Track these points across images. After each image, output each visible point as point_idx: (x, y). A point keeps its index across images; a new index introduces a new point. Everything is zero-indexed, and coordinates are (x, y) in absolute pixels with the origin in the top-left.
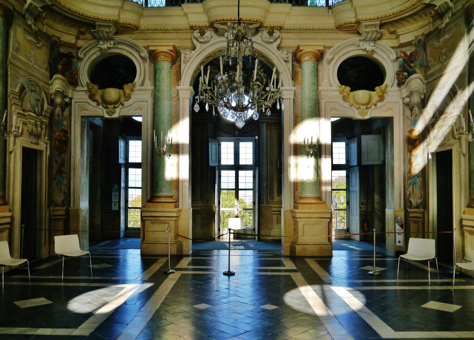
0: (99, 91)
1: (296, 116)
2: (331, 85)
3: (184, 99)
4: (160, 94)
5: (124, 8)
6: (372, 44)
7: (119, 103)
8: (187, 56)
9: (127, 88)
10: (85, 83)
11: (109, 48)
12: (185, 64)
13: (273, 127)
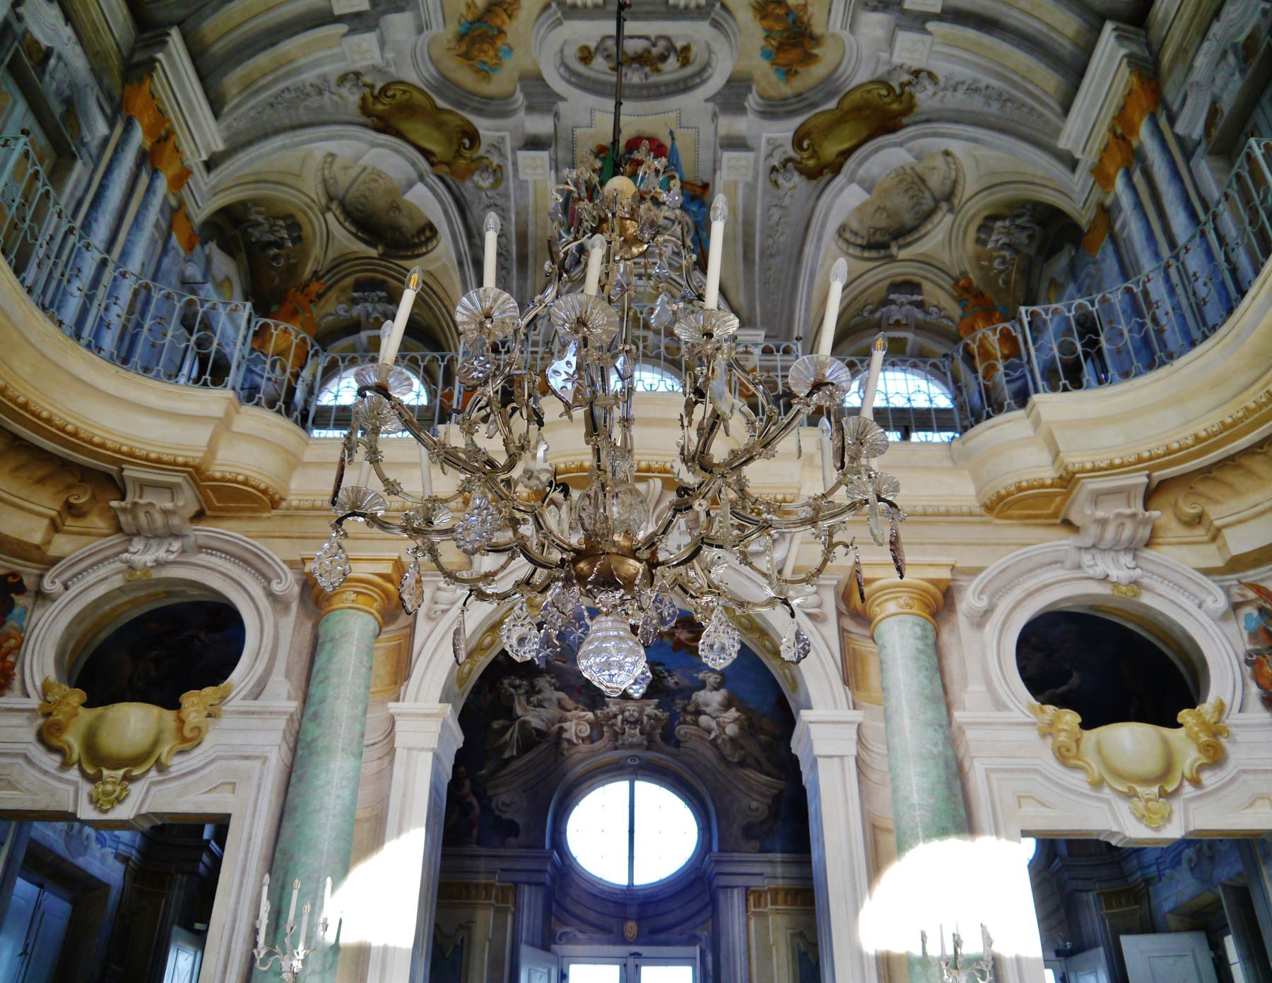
0: (82, 710)
1: (874, 827)
2: (1000, 706)
3: (415, 753)
4: (318, 732)
5: (235, 428)
6: (1126, 559)
7: (152, 761)
8: (442, 595)
9: (194, 702)
10: (38, 683)
11: (159, 564)
12: (433, 624)
13: (770, 906)
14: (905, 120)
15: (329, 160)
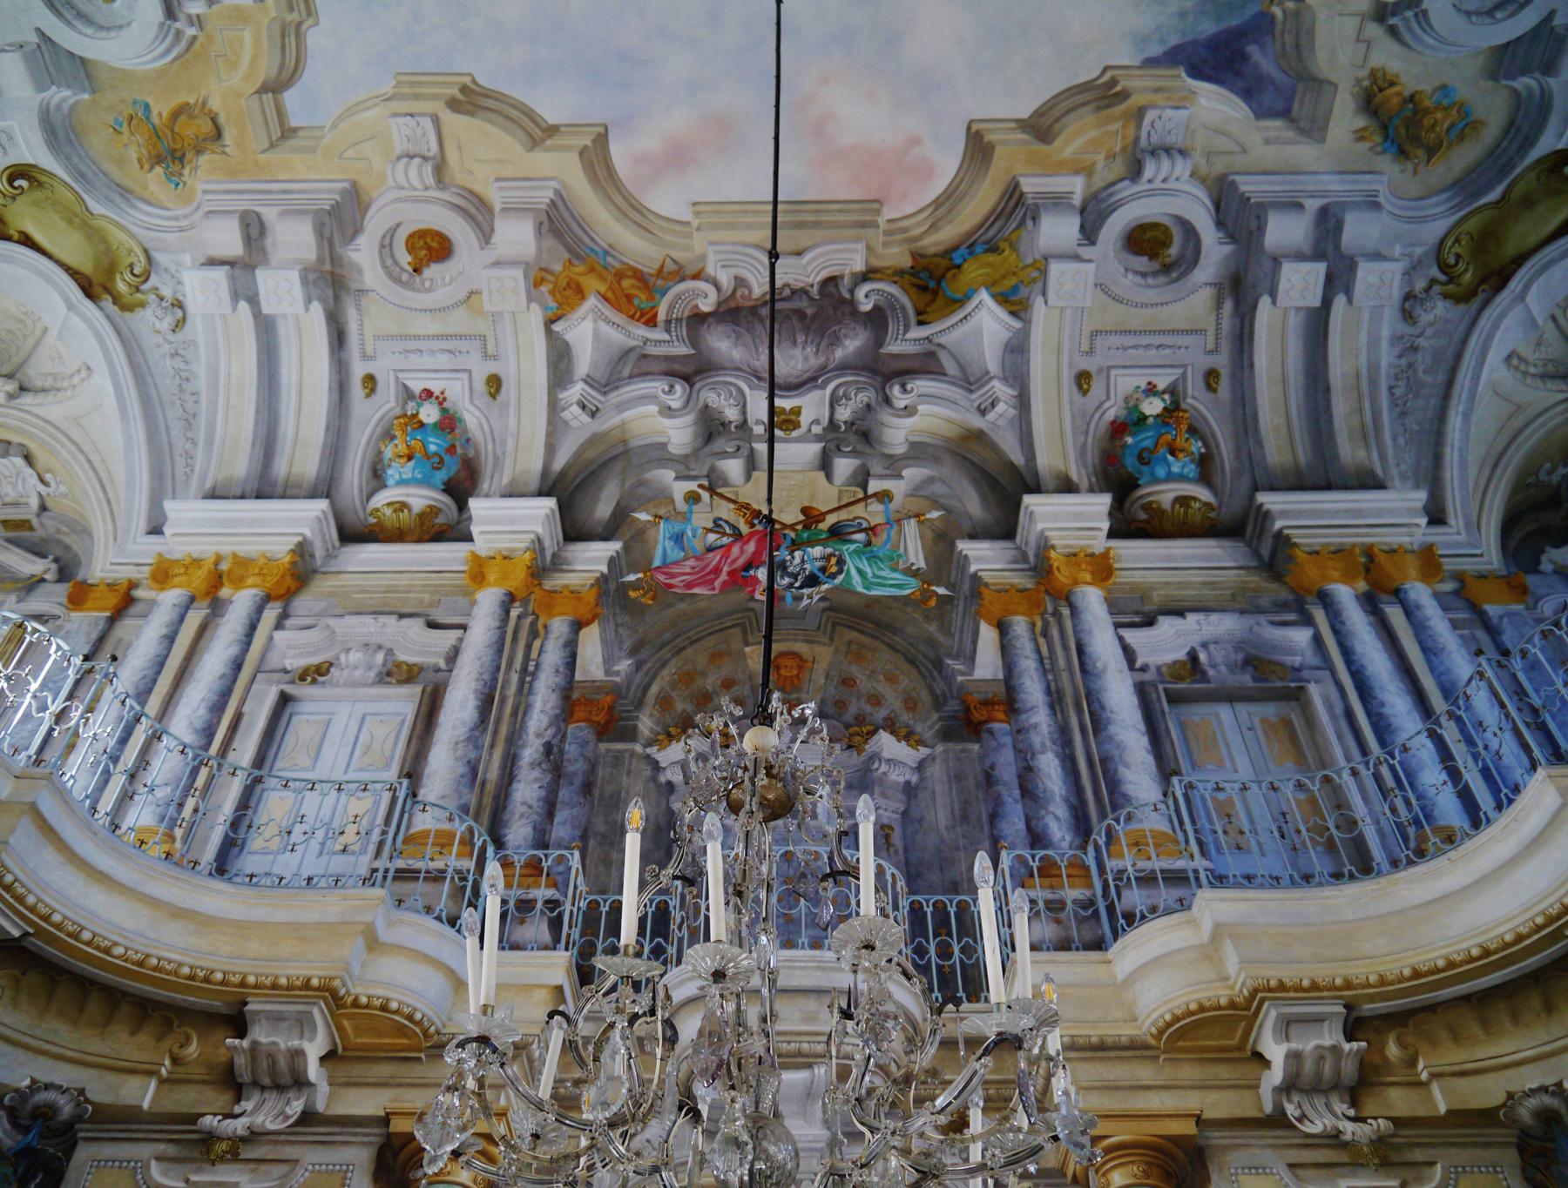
15: (1515, 362)
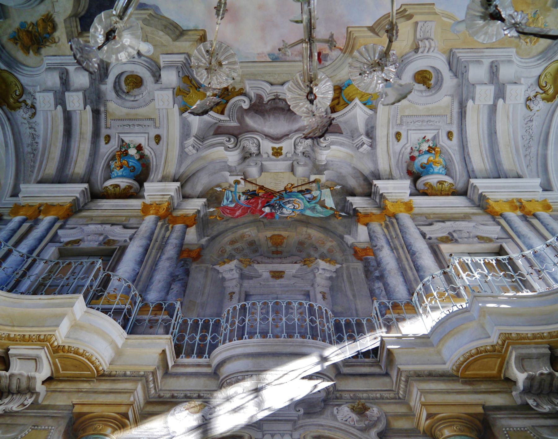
14: (5, 107)
